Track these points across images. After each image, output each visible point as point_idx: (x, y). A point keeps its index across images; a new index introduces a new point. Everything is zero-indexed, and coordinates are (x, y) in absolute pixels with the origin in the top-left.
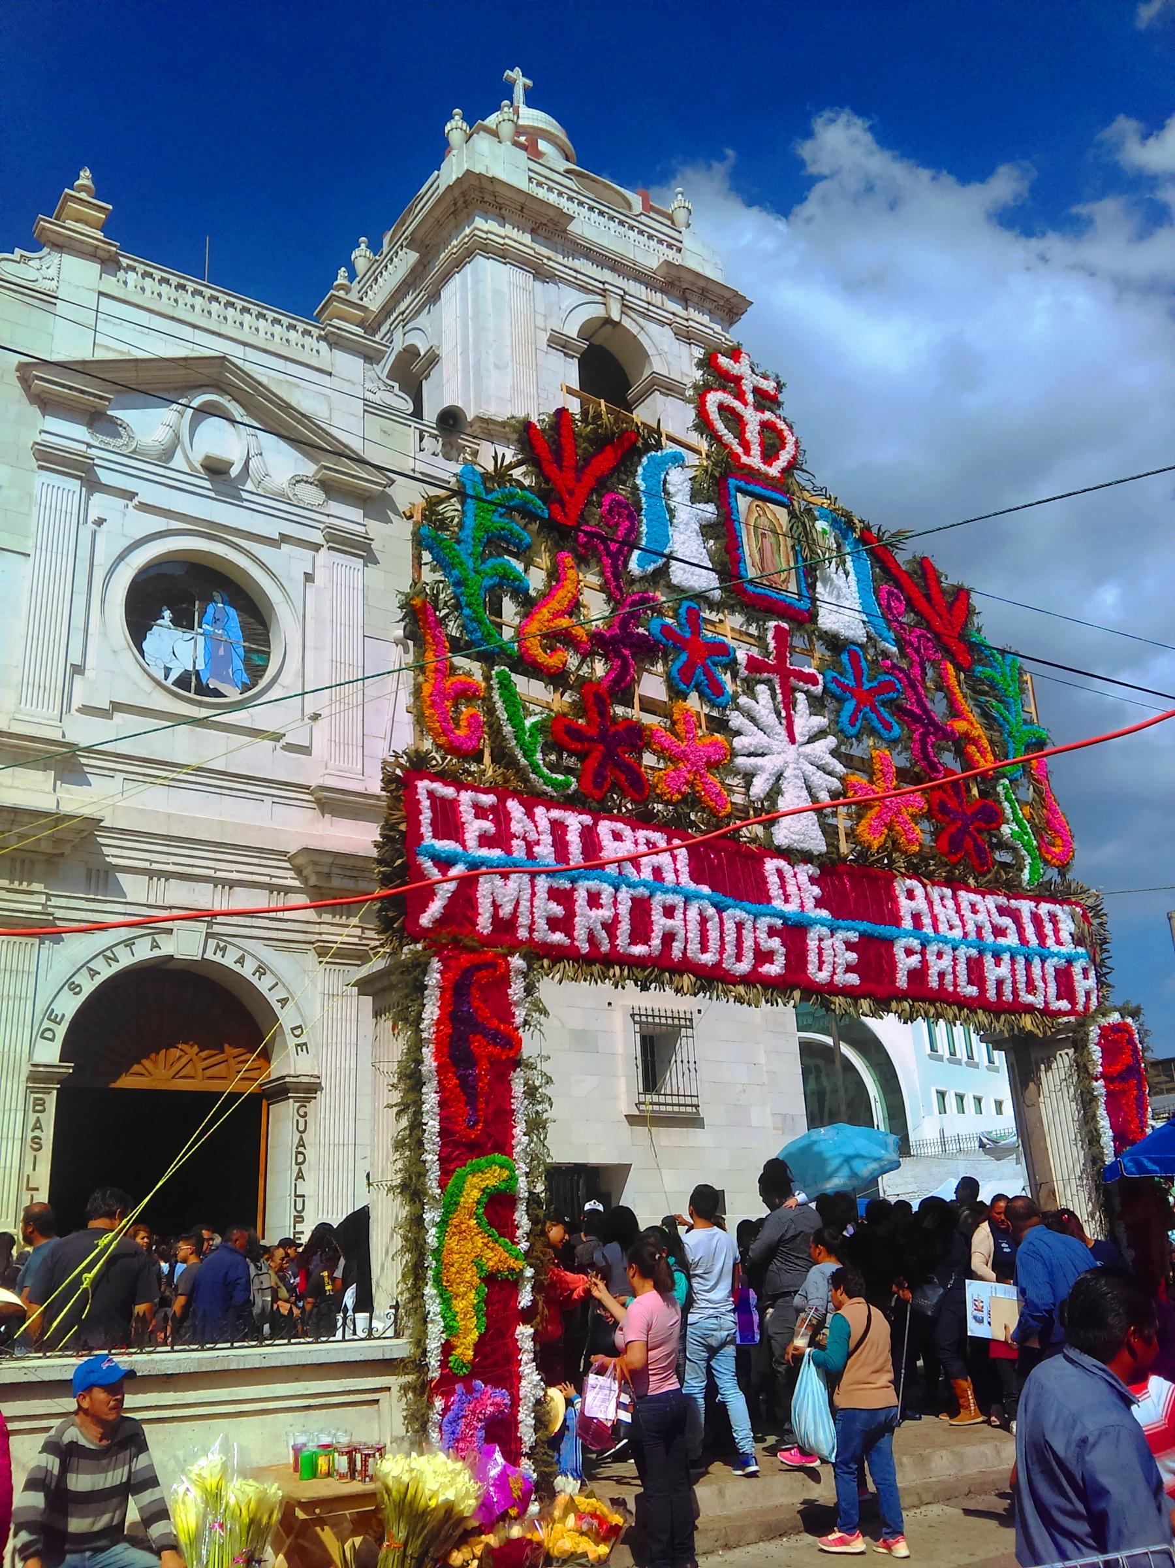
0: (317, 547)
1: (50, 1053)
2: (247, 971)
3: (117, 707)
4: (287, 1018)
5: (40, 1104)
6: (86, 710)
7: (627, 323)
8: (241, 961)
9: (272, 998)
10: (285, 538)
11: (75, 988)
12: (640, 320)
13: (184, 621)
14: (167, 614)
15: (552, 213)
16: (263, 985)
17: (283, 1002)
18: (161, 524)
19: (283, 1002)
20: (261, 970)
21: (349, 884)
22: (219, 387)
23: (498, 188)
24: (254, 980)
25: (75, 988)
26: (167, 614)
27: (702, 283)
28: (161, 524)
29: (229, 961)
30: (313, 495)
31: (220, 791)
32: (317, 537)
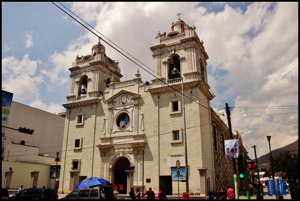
0: (133, 107)
1: (111, 167)
2: (127, 157)
3: (115, 132)
4: (131, 161)
5: (110, 171)
6: (113, 133)
7: (176, 53)
8: (126, 156)
9: (129, 160)
10: (130, 107)
11: (113, 160)
12: (178, 51)
13: (123, 120)
14: (121, 120)
15: (161, 45)
16: (128, 158)
17: (130, 160)
18: (118, 111)
19: (130, 160)
20: (128, 157)
21: (134, 146)
22: (123, 93)
23: (154, 47)
24: (128, 158)
25: (113, 160)
26: (121, 120)
27: (186, 39)
28: (118, 111)
29: (125, 156)
30: (133, 101)
31: (124, 138)
32: (133, 106)
